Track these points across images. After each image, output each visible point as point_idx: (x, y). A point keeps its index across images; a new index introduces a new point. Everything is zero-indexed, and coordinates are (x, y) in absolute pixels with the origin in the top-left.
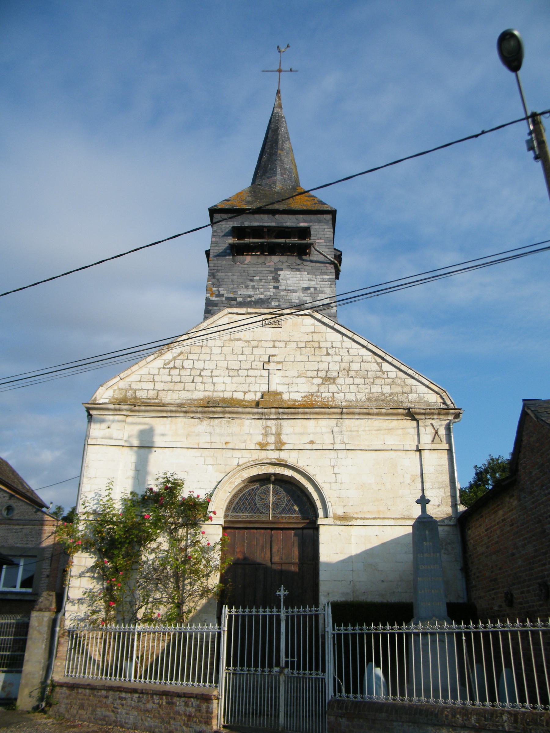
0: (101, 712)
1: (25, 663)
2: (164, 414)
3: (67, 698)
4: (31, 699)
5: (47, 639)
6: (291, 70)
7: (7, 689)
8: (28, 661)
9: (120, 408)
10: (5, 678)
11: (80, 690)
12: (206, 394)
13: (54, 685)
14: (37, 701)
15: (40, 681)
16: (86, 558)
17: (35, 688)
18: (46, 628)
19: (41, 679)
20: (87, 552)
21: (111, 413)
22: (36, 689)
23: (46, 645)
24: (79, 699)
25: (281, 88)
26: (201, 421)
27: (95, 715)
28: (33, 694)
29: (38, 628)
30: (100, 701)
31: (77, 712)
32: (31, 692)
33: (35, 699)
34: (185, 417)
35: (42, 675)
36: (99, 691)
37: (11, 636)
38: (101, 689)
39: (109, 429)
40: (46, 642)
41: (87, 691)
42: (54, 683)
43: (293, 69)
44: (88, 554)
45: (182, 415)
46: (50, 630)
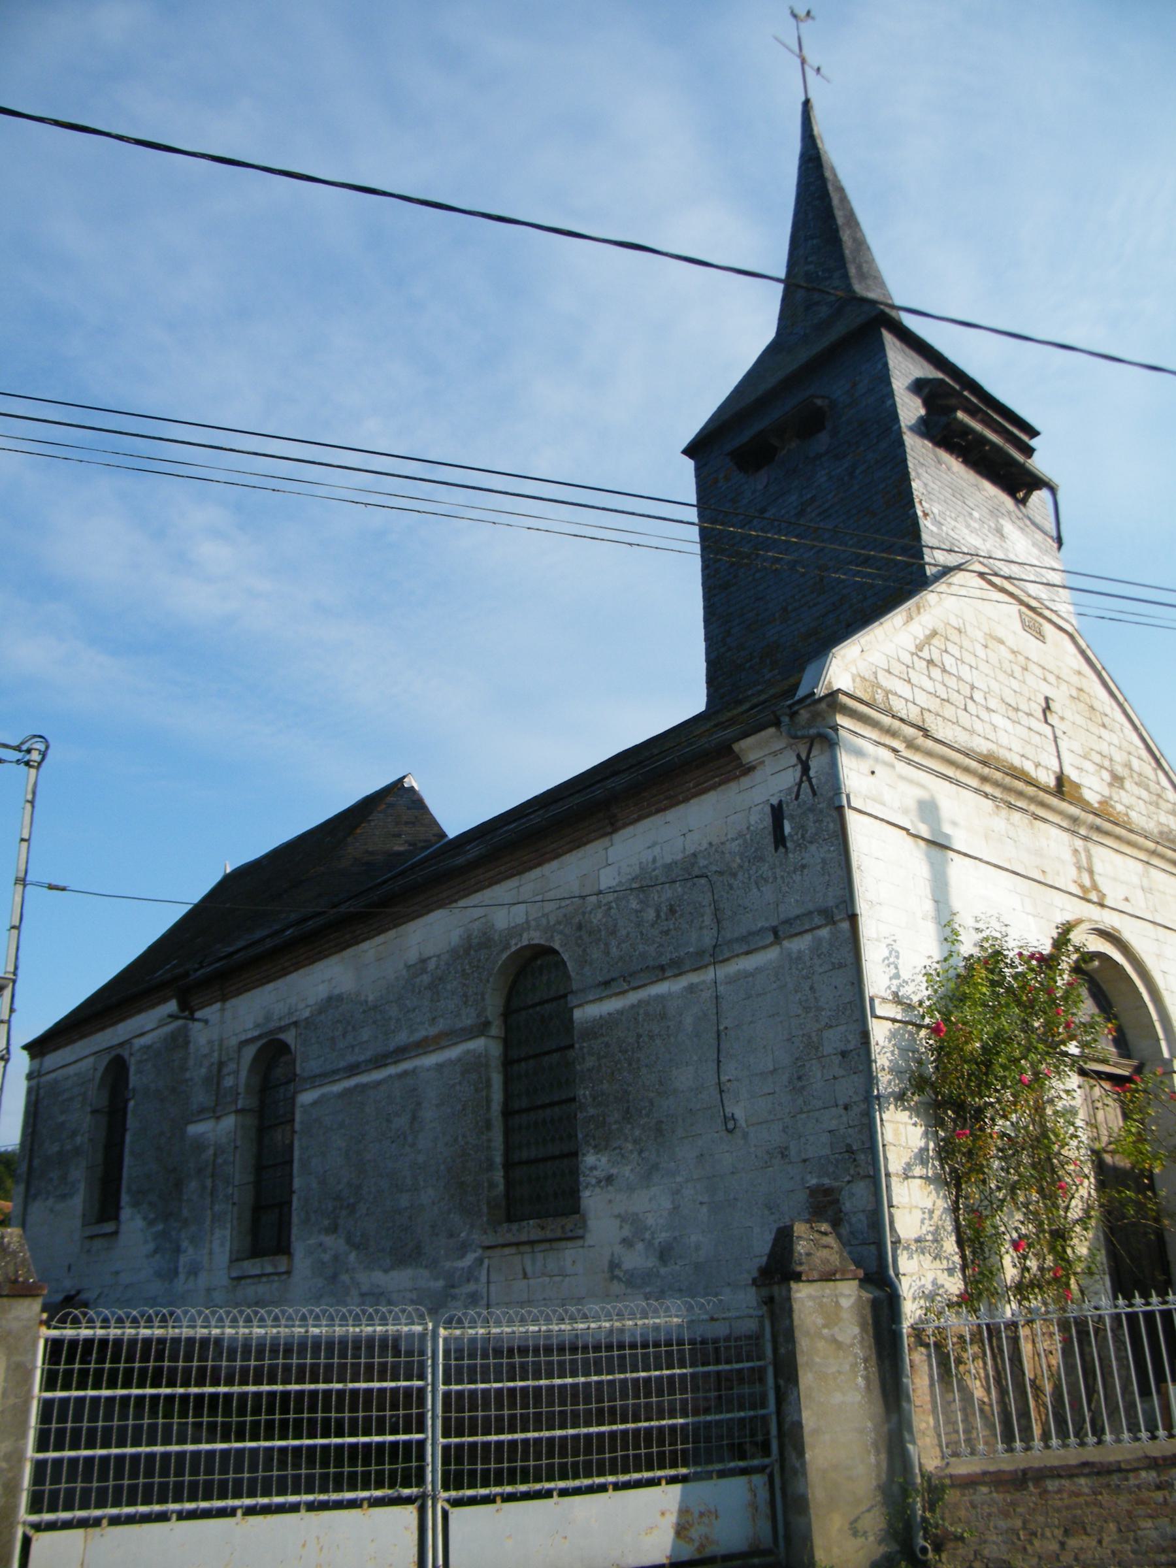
0: (1156, 1529)
1: (808, 1439)
2: (950, 772)
3: (1006, 1515)
4: (861, 1540)
5: (866, 1360)
6: (818, 70)
7: (694, 1533)
8: (816, 1431)
9: (899, 728)
10: (684, 1495)
11: (1051, 1485)
12: (993, 747)
13: (935, 1491)
14: (880, 1542)
15: (874, 1483)
16: (906, 1124)
17: (864, 1508)
18: (856, 1330)
19: (878, 1476)
20: (905, 1109)
21: (874, 734)
22: (868, 1511)
23: (867, 1378)
24: (1058, 1510)
25: (811, 95)
26: (997, 807)
27: (1136, 1541)
28: (860, 1525)
29: (825, 1331)
30: (1140, 1502)
31: (1062, 1544)
32: (856, 1521)
33: (871, 1539)
34: (977, 791)
35: (878, 1464)
36: (1131, 1475)
37: (682, 1365)
38: (1135, 1470)
39: (872, 778)
40: (866, 1368)
41: (1082, 1481)
42: (935, 1481)
43: (822, 70)
44: (907, 1113)
45: (974, 782)
46: (871, 1332)
